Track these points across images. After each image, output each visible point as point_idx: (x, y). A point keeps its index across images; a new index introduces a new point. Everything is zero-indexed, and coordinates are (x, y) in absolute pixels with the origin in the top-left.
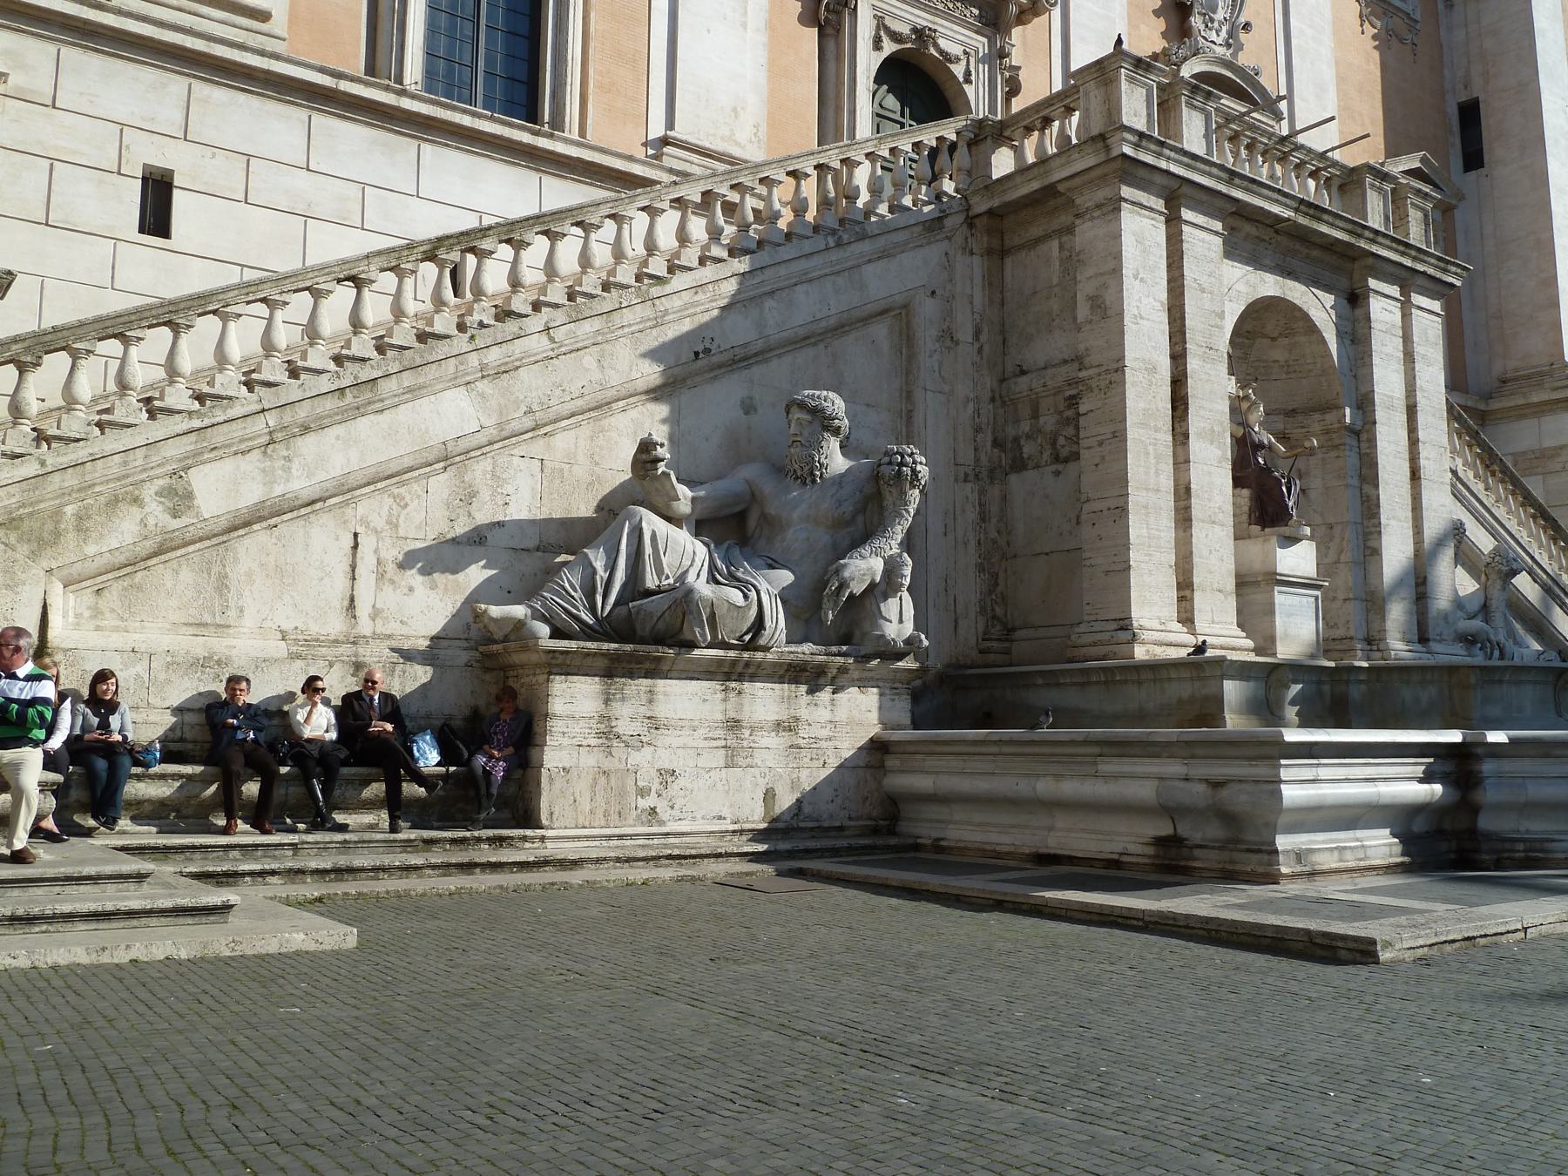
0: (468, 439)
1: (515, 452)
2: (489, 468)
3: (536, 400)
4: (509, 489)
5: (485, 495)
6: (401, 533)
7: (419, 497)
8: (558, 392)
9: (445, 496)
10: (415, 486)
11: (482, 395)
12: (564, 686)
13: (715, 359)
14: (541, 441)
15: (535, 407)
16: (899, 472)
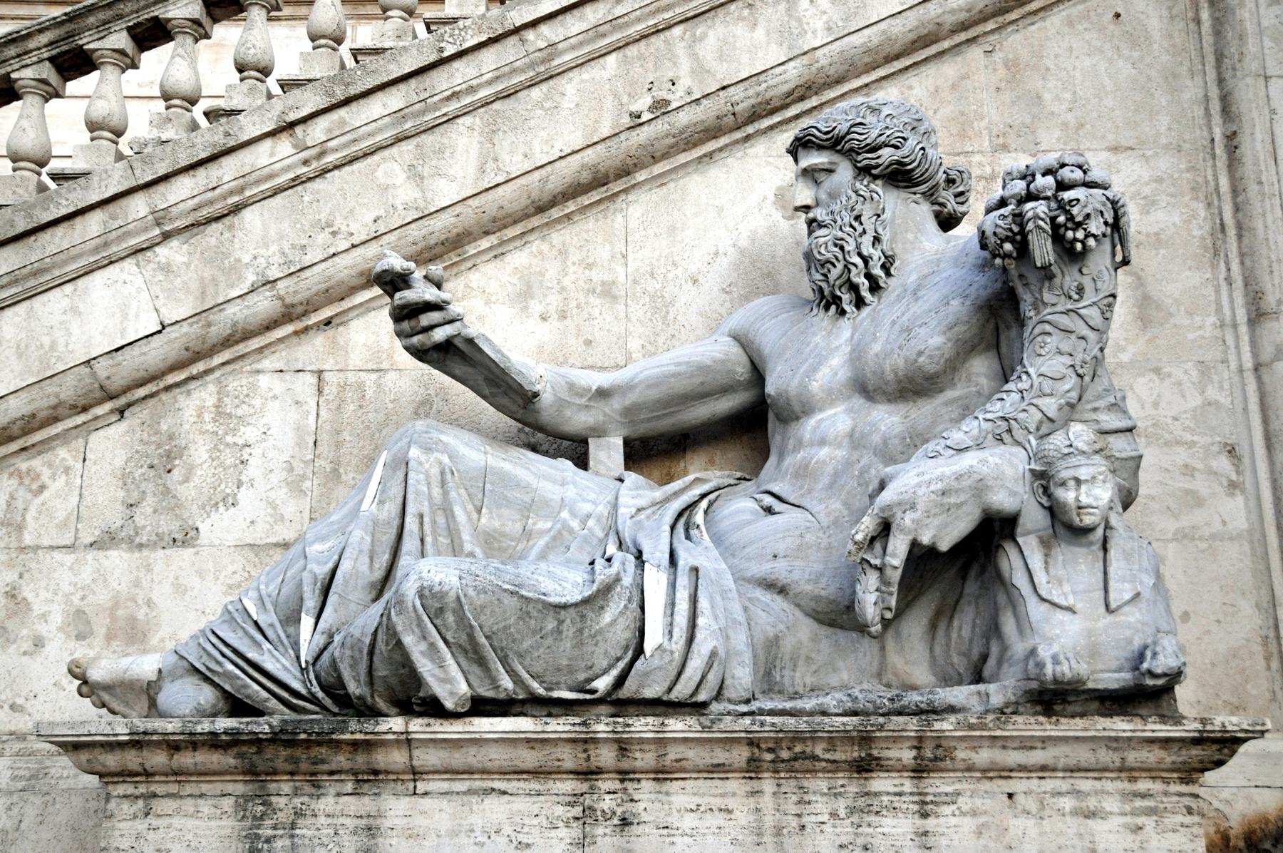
0: (136, 350)
1: (267, 363)
2: (211, 402)
3: (277, 259)
4: (249, 433)
5: (200, 452)
6: (28, 539)
7: (67, 470)
8: (322, 238)
9: (119, 462)
10: (62, 453)
11: (166, 269)
12: (141, 825)
13: (683, 118)
14: (319, 340)
15: (274, 273)
16: (1018, 217)
